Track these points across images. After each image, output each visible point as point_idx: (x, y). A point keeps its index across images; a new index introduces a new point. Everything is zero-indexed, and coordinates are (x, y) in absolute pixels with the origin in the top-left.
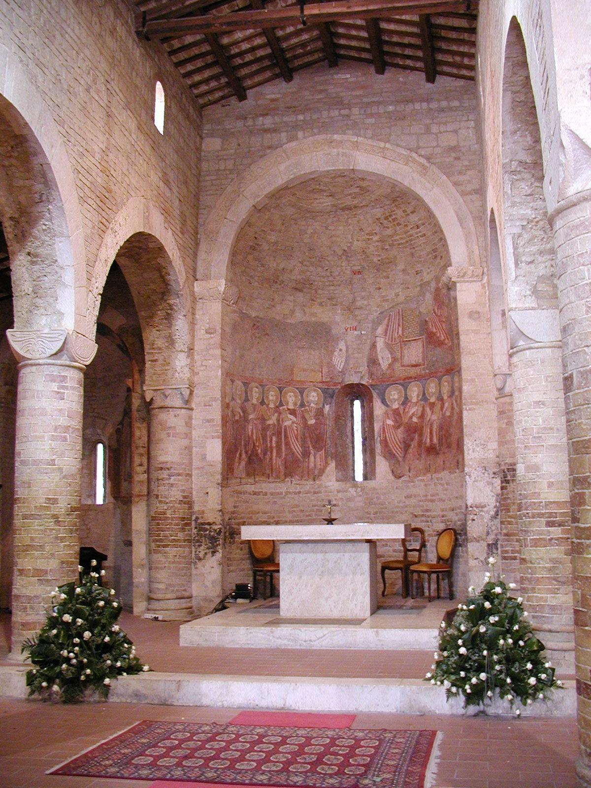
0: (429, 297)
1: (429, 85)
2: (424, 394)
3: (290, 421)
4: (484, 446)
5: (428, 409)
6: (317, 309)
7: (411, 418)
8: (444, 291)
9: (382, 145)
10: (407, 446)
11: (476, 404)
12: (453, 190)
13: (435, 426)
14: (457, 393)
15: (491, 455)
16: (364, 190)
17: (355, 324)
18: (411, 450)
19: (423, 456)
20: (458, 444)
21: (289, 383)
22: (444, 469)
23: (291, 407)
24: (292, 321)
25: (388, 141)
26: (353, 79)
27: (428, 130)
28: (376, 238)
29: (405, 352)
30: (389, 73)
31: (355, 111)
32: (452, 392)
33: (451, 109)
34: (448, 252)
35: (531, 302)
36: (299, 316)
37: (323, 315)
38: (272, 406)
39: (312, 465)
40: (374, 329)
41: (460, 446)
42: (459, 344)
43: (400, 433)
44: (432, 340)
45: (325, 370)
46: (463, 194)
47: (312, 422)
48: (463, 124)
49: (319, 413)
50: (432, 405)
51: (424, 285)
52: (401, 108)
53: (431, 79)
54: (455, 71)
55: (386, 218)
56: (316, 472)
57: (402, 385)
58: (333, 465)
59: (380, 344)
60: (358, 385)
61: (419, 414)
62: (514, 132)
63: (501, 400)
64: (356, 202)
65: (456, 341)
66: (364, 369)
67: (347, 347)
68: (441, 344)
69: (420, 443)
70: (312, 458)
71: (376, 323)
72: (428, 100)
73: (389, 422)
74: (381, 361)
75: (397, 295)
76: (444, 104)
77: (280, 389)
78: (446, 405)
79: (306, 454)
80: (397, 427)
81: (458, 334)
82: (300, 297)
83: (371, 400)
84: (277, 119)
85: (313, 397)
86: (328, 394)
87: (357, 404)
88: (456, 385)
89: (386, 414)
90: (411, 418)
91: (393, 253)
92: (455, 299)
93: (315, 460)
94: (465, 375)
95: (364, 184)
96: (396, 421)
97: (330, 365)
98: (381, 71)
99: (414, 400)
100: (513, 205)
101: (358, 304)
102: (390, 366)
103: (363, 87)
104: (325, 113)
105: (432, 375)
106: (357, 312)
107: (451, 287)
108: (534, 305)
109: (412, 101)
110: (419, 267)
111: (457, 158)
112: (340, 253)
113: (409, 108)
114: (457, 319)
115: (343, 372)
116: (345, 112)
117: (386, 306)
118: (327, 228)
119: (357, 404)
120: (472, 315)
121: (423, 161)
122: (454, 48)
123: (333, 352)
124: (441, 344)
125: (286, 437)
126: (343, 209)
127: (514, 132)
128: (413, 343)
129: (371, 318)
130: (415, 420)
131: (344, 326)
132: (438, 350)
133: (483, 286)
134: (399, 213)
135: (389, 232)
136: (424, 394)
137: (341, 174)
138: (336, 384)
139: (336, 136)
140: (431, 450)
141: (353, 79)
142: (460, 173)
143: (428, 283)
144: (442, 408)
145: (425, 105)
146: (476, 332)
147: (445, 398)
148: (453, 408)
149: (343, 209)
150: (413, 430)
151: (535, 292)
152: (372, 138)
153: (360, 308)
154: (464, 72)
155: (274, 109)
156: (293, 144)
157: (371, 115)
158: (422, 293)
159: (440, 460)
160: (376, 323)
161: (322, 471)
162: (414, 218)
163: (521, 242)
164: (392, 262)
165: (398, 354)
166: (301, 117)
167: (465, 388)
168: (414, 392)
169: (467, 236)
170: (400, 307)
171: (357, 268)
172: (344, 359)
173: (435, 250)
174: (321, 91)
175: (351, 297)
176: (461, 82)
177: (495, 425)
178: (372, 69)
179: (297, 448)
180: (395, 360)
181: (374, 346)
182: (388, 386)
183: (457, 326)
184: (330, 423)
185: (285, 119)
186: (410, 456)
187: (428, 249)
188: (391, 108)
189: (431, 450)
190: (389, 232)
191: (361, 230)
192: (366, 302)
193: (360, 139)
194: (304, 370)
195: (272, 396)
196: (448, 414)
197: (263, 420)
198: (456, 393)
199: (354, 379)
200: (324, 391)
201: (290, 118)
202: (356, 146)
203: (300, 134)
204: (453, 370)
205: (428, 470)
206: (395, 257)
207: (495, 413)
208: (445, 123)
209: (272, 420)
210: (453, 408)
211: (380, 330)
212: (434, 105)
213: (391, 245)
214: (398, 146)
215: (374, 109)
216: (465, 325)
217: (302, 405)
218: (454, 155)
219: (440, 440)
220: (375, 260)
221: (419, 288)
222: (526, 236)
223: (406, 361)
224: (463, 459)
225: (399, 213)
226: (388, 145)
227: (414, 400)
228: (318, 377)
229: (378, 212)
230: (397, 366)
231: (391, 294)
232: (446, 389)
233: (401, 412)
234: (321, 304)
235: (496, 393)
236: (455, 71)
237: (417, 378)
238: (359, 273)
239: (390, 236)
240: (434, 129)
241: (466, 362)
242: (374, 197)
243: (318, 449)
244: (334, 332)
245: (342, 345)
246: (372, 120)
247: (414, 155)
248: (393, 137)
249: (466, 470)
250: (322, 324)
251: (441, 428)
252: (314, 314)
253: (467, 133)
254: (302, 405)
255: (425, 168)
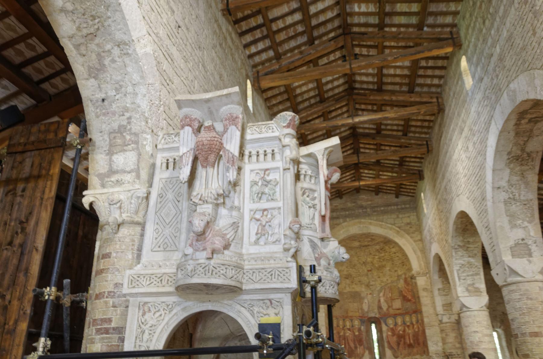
0: (402, 282)
1: (396, 199)
2: (404, 322)
3: (348, 333)
4: (437, 344)
5: (407, 328)
6: (354, 286)
7: (399, 331)
8: (409, 279)
9: (381, 223)
10: (398, 344)
11: (430, 326)
12: (411, 240)
13: (411, 335)
14: (420, 322)
15: (440, 349)
16: (373, 240)
17: (370, 292)
18: (401, 346)
19: (407, 348)
20: (424, 343)
21: (347, 317)
22: (417, 354)
23: (348, 327)
24: (345, 291)
25: (382, 222)
26: (366, 198)
27: (398, 217)
28: (377, 257)
29: (393, 304)
30: (380, 195)
31: (368, 210)
32: (417, 321)
33: (406, 208)
34: (410, 264)
35: (466, 294)
36: (348, 289)
37: (357, 288)
38: (341, 327)
39: (359, 352)
40: (379, 294)
41: (425, 345)
42: (419, 302)
43: (395, 339)
44: (405, 299)
45: (360, 311)
46: (415, 241)
47: (357, 333)
48: (412, 214)
49: (359, 330)
50: (408, 326)
51: (399, 276)
52: (386, 208)
53: (397, 197)
54: (406, 194)
55: (381, 249)
56: (361, 355)
57: (394, 317)
58: (367, 352)
59: (382, 300)
60: (375, 317)
61: (403, 330)
62: (456, 236)
63: (442, 325)
64: (369, 244)
65: (417, 300)
66: (376, 311)
67: (368, 301)
68: (409, 300)
69: (405, 343)
70: (358, 349)
71: (380, 291)
72: (397, 205)
73: (390, 333)
74: (383, 307)
75: (387, 280)
76: (403, 206)
77: (344, 320)
78: (415, 326)
79: (356, 348)
80: (394, 334)
81: (419, 297)
82: (348, 281)
83: (380, 323)
84: (338, 213)
85: (356, 323)
86: (362, 321)
87: (373, 326)
88: (419, 318)
89: (388, 330)
90: (399, 331)
91: (384, 263)
92: (416, 283)
93: (359, 350)
94: (425, 314)
95: (373, 237)
96: (392, 333)
97: (362, 309)
98: (377, 194)
99: (400, 324)
100: (456, 259)
101: (372, 283)
102: (388, 309)
103: (371, 201)
104: (357, 211)
105: (407, 313)
106: (371, 287)
107: (413, 278)
108: (468, 295)
109: (390, 205)
110: (396, 269)
111: (411, 227)
112: (362, 263)
113: (390, 208)
114: (418, 291)
115: (367, 312)
116: (364, 210)
117: (383, 284)
118: (356, 253)
119: (373, 326)
120: (425, 289)
121: (398, 229)
122: (408, 187)
123: (362, 304)
124: (409, 300)
125: (348, 340)
126: (363, 246)
127: (456, 236)
128: (397, 300)
129: (377, 289)
130: (401, 332)
131: (366, 293)
132: (409, 303)
133: (427, 278)
134: (387, 248)
135: (383, 255)
136: (404, 322)
137: (364, 234)
138: (365, 317)
139: (363, 220)
140: (410, 346)
141: (366, 198)
142: (413, 233)
143: (401, 275)
144: (413, 327)
145: (396, 207)
146: (426, 297)
147: (414, 323)
148: (419, 328)
149: (363, 246)
150: (401, 337)
151: (467, 290)
152: (376, 220)
153: (372, 285)
154: (410, 194)
155: (337, 209)
156: (346, 223)
157: (375, 211)
158: (398, 279)
159: (415, 350)
160: (380, 291)
161: (363, 355)
162: (393, 250)
163: (460, 272)
164: (384, 266)
165: (390, 305)
166: (347, 213)
167: (426, 320)
168: (399, 320)
169: (418, 258)
170: (389, 285)
171: (369, 269)
172: (367, 307)
173: (403, 262)
174: (354, 202)
175: (368, 281)
176: (409, 198)
177: (440, 335)
178: (374, 194)
179: (352, 345)
180: (389, 307)
181: (379, 301)
182: (387, 318)
183: (418, 294)
184: (364, 334)
185: (341, 213)
186: (400, 348)
187: (400, 262)
188: (382, 208)
189: (410, 346)
190: (383, 255)
191: (371, 254)
192: (374, 283)
193: (372, 221)
194: (352, 312)
195: (341, 323)
196: (417, 330)
197: (339, 333)
198: (420, 322)
199: (372, 315)
200: (361, 320)
201: (343, 213)
202: (370, 223)
203: (348, 219)
204: (418, 311)
205: (409, 355)
206: (385, 265)
207: (439, 331)
208: (404, 214)
209: (342, 334)
210: (419, 328)
211: (381, 294)
212: (399, 207)
213: (383, 260)
214: (387, 223)
215: (376, 209)
216: (422, 294)
217: (353, 326)
218: (409, 226)
219: (414, 341)
220: (377, 265)
221: (396, 278)
222: (462, 270)
223: (394, 307)
224: (428, 350)
225: (387, 248)
226: (383, 223)
227: (400, 324)
228: (357, 314)
229: (378, 247)
230: (390, 309)
231: (385, 280)
232: (414, 320)
233: (394, 328)
234: (356, 284)
235: (439, 322)
236: (406, 194)
237: (400, 314)
238: (370, 271)
239: (383, 256)
240: (400, 216)
241: (424, 309)
242: (376, 242)
243: (360, 345)
244: (362, 295)
245: (366, 301)
246: (375, 213)
247: (394, 227)
248: (384, 220)
249: (430, 354)
250: (357, 292)
251: (414, 336)
252: (353, 288)
253: (413, 218)
254: (353, 326)
255: (398, 232)
